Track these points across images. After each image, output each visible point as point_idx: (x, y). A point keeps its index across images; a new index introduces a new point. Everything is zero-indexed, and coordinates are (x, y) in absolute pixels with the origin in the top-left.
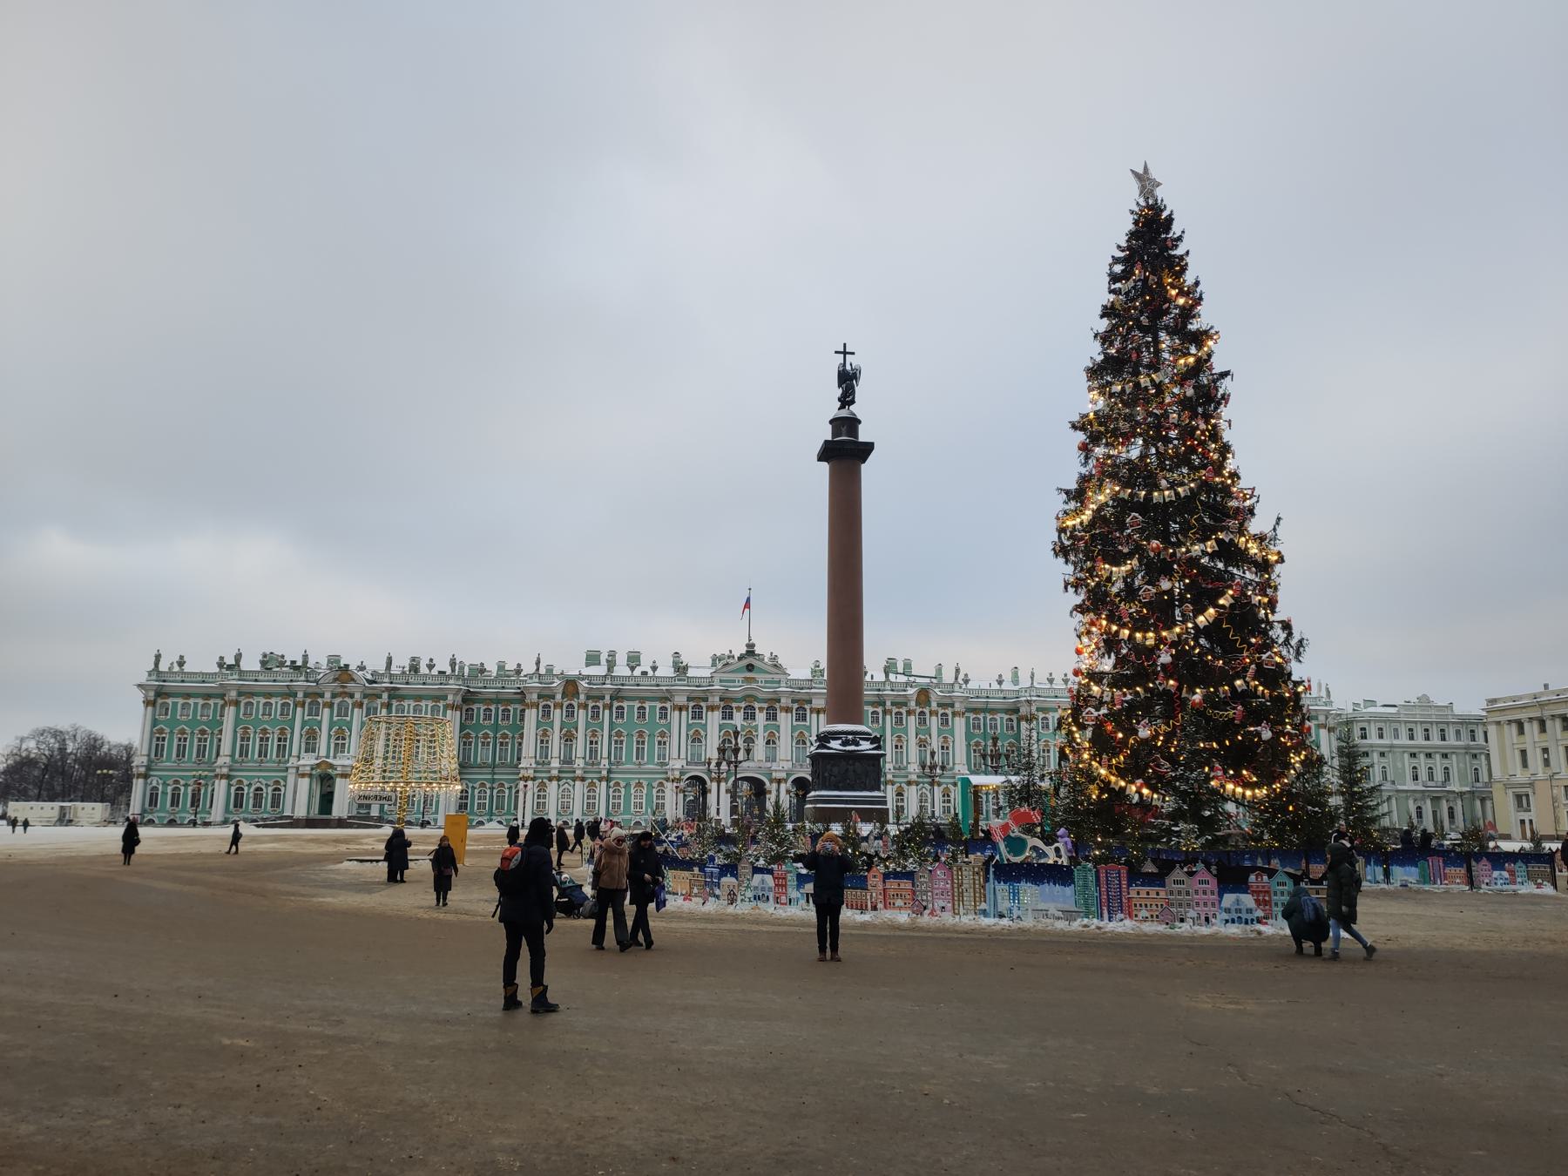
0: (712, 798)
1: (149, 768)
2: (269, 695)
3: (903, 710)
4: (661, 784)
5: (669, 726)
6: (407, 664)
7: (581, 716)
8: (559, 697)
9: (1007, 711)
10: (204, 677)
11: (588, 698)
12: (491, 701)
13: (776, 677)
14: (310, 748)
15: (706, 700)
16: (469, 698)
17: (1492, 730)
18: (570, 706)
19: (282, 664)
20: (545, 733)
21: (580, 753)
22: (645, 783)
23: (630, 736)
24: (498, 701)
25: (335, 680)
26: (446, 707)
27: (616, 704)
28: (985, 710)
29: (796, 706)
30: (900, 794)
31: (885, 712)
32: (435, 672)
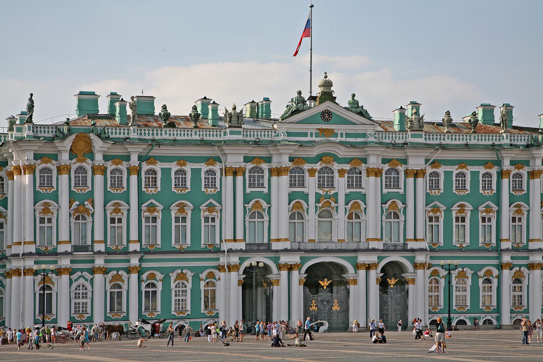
0: (279, 293)
3: (524, 172)
4: (211, 275)
5: (218, 197)
8: (65, 157)
11: (106, 158)
13: (359, 129)
15: (268, 160)
18: (81, 170)
20: (46, 210)
21: (99, 236)
22: (189, 275)
23: (167, 210)
27: (145, 167)
29: (386, 167)
30: (517, 280)
31: (501, 174)
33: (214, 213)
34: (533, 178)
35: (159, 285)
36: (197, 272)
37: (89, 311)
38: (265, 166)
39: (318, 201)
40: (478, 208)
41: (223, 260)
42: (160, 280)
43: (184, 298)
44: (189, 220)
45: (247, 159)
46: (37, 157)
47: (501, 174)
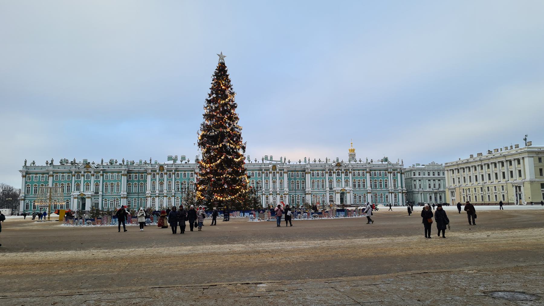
1: (25, 197)
2: (64, 173)
6: (108, 161)
7: (165, 177)
9: (301, 171)
10: (42, 167)
11: (167, 171)
12: (137, 173)
14: (78, 189)
16: (129, 172)
17: (446, 172)
19: (67, 163)
20: (154, 182)
24: (139, 173)
25: (85, 167)
26: (122, 175)
28: (295, 171)
32: (118, 164)
46: (152, 171)
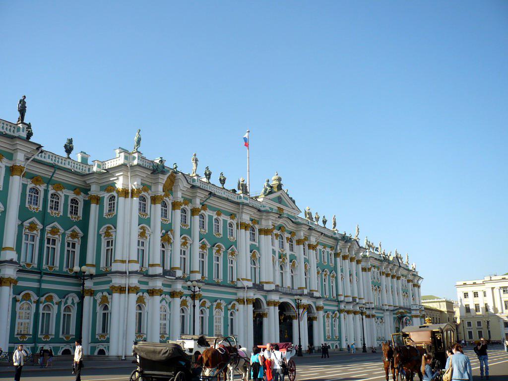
8: (160, 188)
22: (224, 304)
26: (12, 170)
31: (336, 255)
33: (234, 257)
34: (344, 260)
35: (207, 311)
36: (229, 302)
37: (167, 332)
38: (257, 227)
39: (280, 258)
40: (330, 274)
41: (241, 294)
42: (208, 308)
43: (219, 324)
44: (221, 259)
45: (252, 220)
47: (336, 255)
